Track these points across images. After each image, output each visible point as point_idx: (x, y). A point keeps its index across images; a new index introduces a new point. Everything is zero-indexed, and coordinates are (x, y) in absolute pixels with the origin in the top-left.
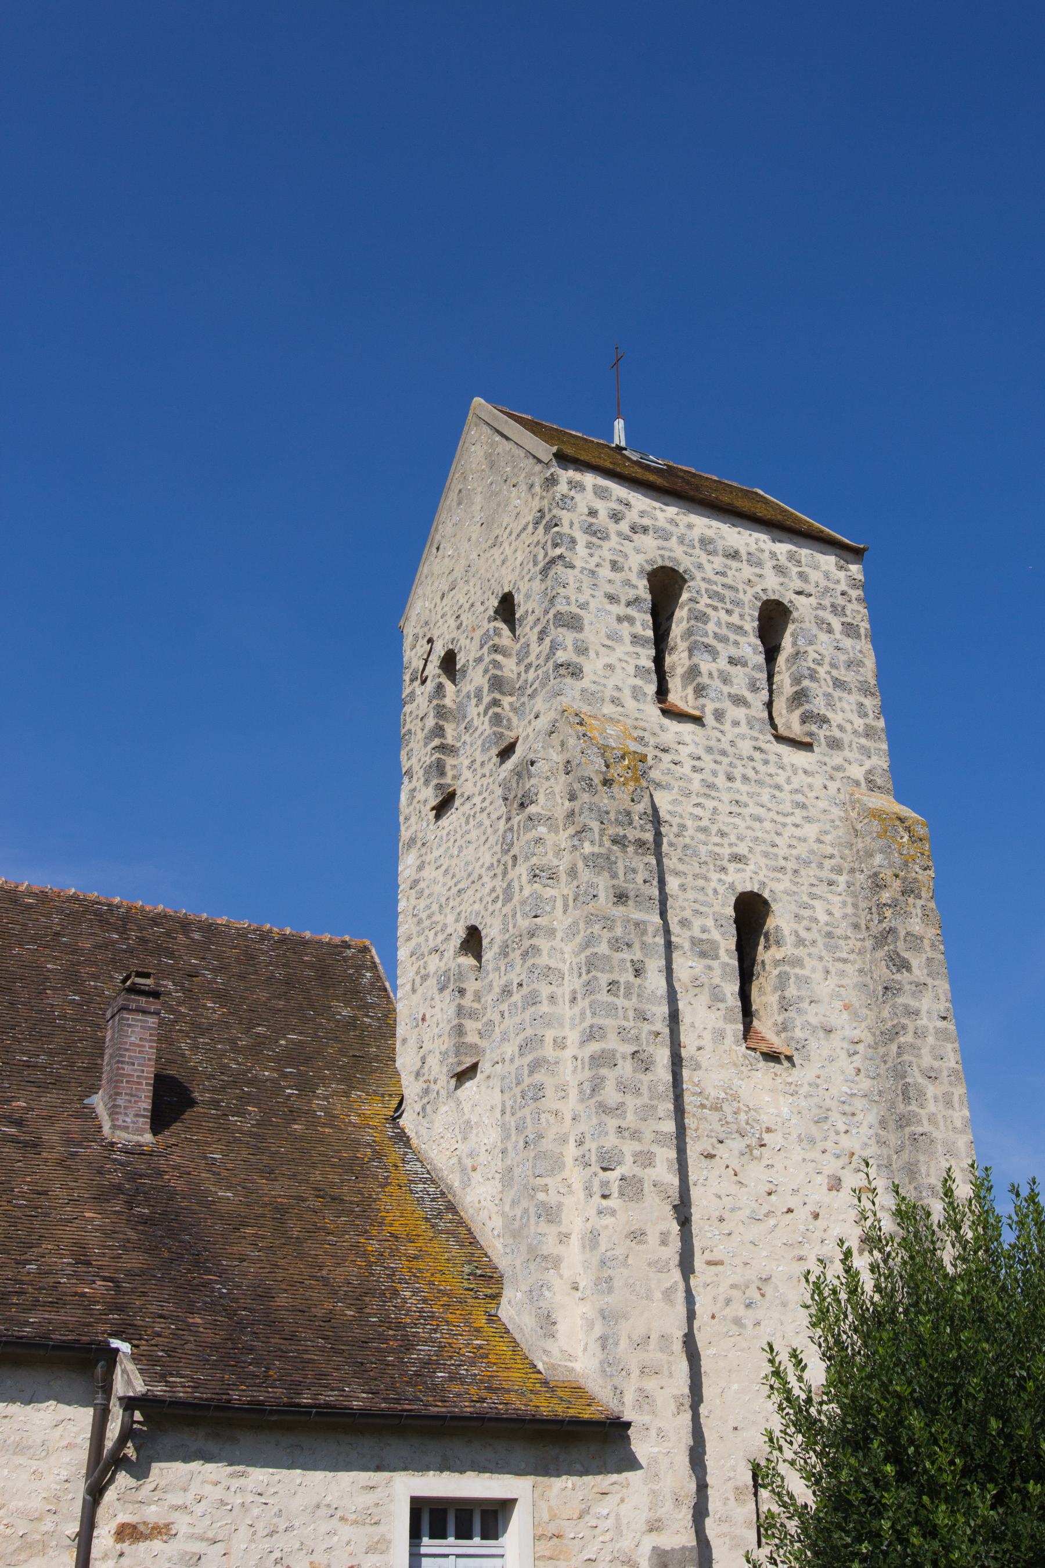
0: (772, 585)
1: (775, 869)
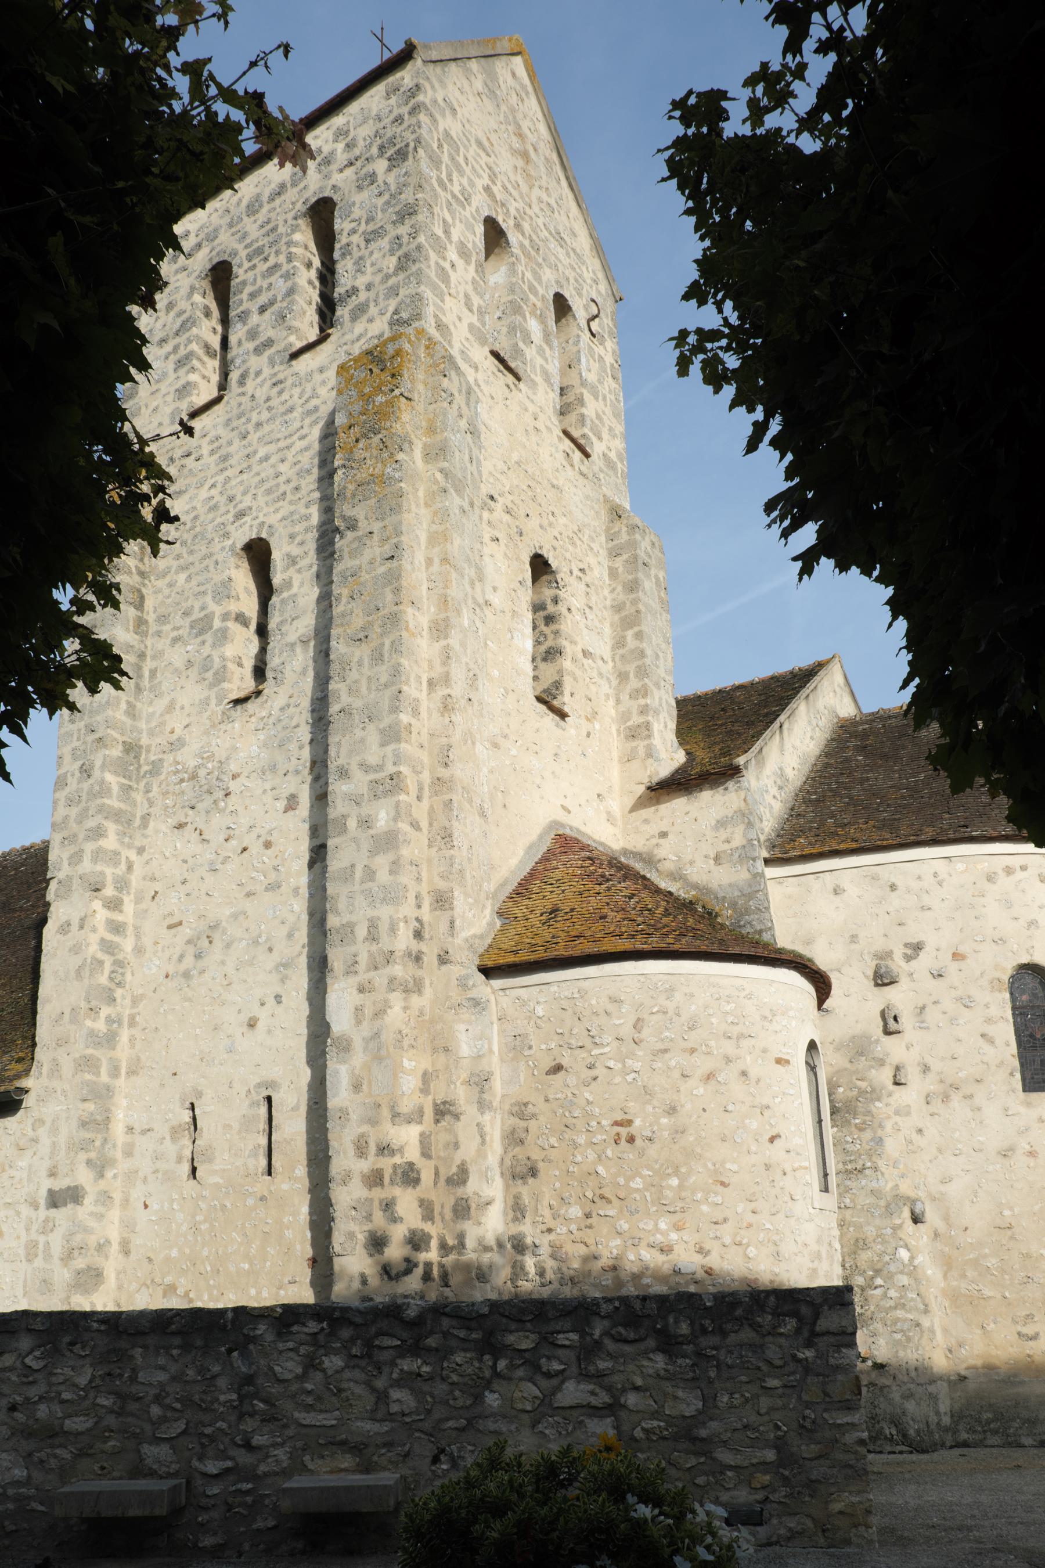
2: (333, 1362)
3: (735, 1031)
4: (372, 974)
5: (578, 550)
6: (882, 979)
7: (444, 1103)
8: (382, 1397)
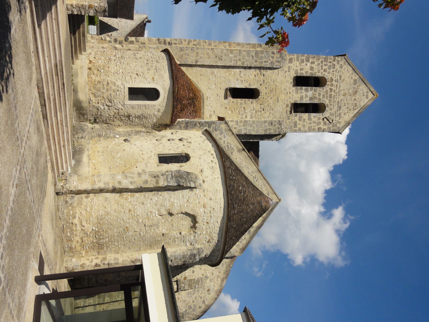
3: (158, 68)
5: (267, 108)
6: (180, 140)
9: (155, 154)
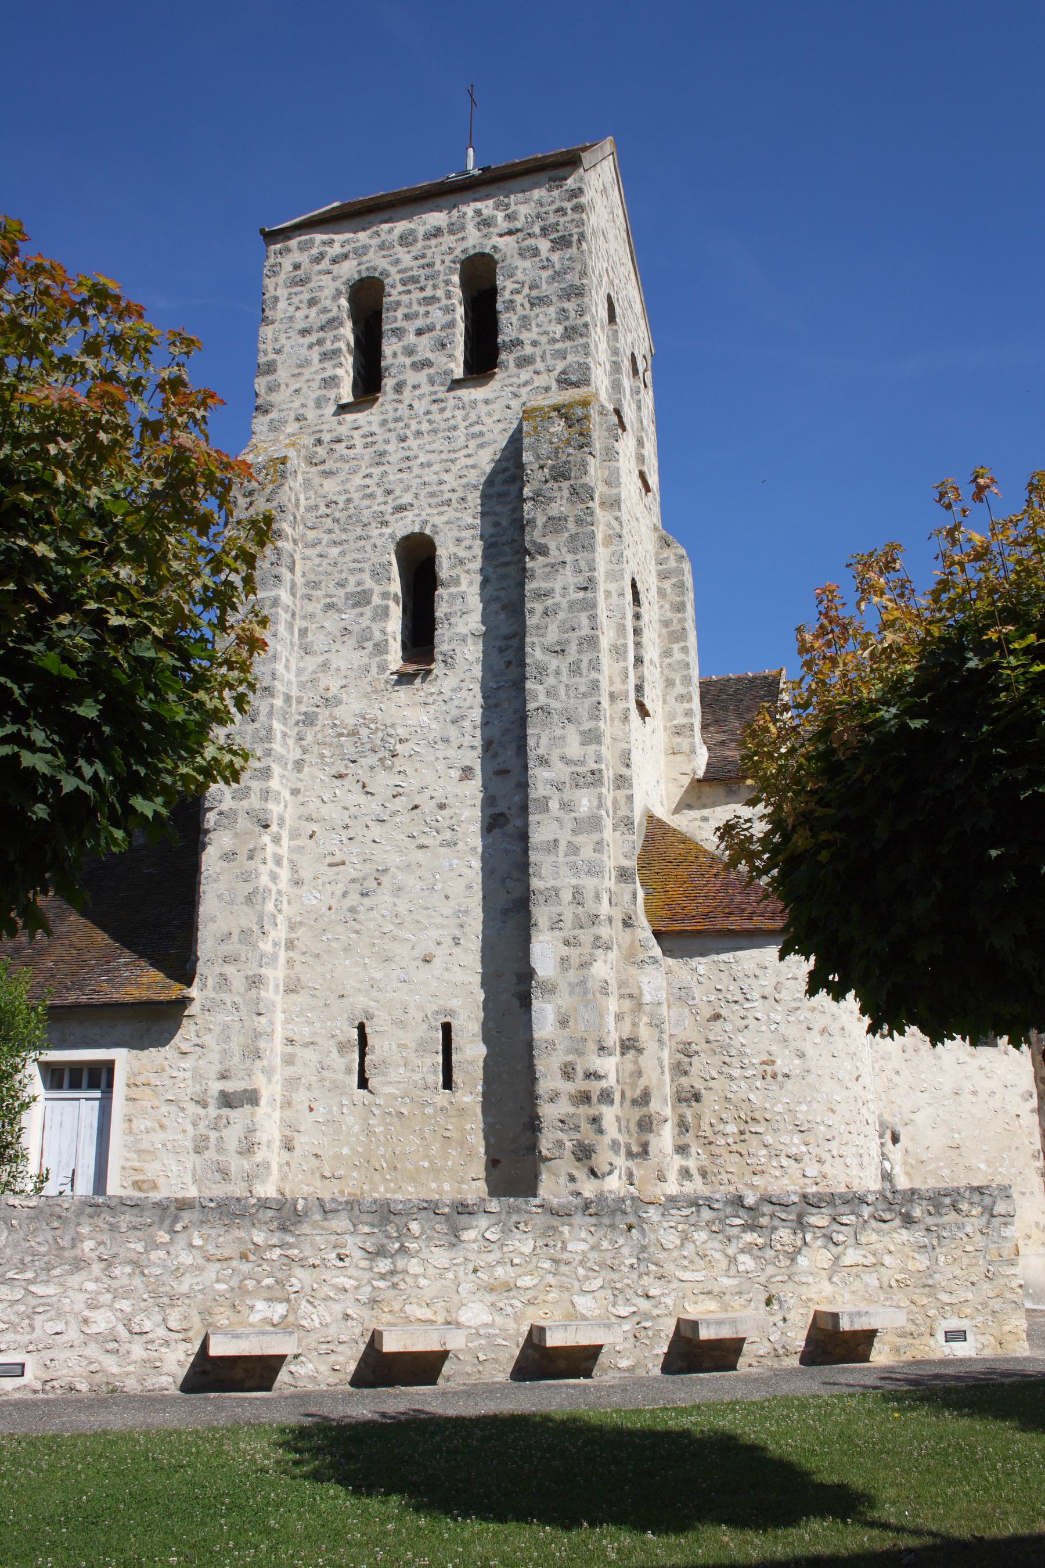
0: (473, 240)
1: (443, 504)
2: (701, 1236)
4: (577, 932)
7: (629, 1039)
8: (733, 1260)
9: (973, 1056)
